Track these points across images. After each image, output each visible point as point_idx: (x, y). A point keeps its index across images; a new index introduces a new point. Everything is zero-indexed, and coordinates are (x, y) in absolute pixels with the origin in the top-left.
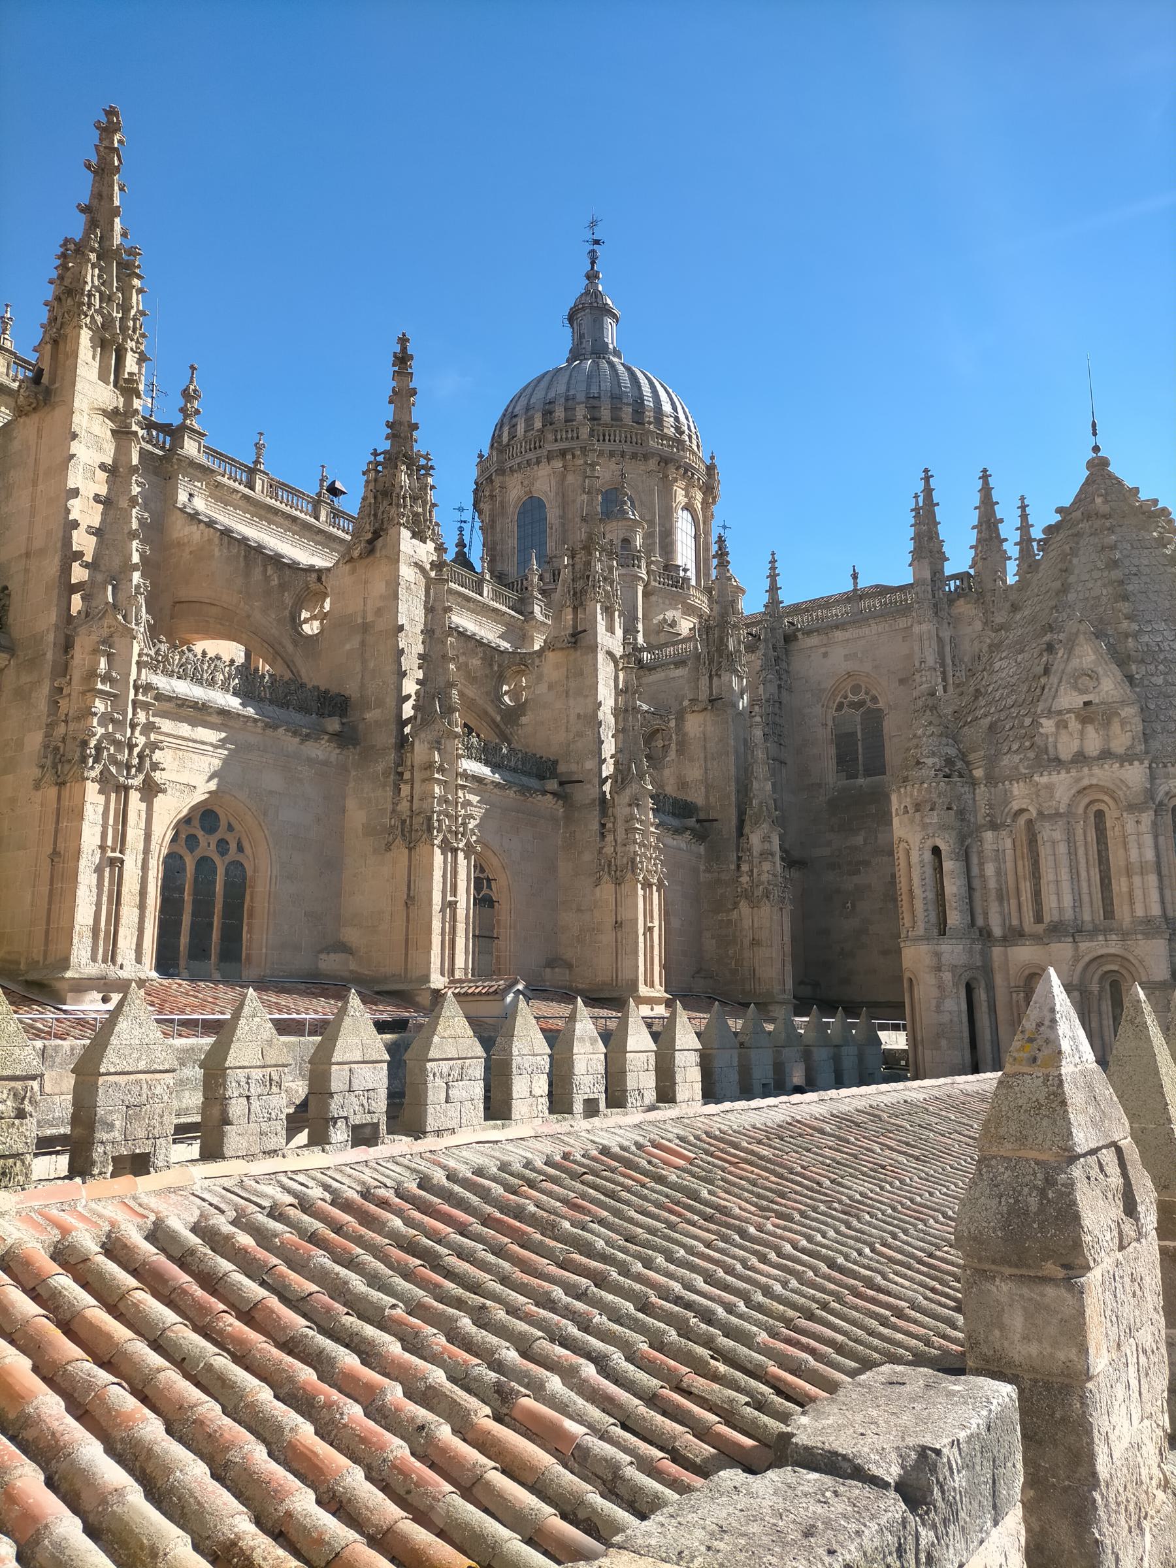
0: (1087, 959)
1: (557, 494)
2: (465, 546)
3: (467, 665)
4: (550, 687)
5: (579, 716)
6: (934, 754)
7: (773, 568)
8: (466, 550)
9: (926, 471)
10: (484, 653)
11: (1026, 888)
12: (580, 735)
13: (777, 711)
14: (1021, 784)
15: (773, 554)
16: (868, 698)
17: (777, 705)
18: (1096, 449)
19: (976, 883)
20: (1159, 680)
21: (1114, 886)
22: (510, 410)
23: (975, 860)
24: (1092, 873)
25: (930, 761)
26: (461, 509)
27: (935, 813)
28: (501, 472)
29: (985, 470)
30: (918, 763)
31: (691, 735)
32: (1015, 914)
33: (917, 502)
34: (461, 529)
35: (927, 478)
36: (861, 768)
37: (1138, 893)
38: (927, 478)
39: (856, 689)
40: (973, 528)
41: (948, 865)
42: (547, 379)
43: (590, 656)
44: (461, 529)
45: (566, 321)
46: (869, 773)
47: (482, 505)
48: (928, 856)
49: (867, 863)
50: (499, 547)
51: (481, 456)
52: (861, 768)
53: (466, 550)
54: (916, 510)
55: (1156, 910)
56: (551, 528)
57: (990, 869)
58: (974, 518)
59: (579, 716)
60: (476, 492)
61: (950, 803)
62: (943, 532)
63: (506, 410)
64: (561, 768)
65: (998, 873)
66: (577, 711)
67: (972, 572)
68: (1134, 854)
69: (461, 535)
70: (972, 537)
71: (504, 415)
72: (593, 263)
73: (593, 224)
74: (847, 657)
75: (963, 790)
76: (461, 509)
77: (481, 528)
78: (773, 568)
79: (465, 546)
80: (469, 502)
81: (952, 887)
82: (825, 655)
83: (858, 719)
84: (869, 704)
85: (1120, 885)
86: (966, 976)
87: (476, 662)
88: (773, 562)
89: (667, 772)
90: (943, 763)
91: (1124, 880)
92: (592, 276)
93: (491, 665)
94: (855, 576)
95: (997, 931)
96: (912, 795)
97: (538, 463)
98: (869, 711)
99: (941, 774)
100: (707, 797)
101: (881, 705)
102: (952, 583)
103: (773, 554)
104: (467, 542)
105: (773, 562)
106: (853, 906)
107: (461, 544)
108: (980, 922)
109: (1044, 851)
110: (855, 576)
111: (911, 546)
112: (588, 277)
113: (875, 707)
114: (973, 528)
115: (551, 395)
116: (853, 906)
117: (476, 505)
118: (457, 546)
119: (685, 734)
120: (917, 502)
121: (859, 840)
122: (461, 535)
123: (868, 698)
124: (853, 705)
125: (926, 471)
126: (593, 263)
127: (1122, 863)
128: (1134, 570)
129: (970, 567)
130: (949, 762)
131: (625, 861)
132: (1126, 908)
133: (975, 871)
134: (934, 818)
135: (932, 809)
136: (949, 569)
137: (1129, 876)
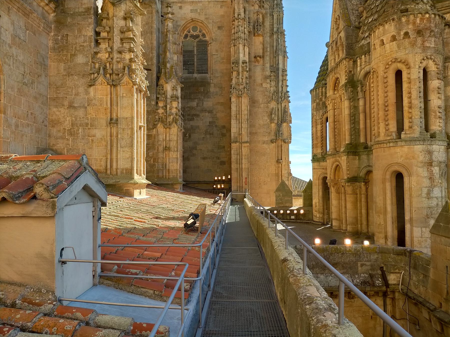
16: (200, 34)
36: (195, 69)
39: (195, 29)
46: (199, 72)
49: (198, 116)
52: (195, 69)
83: (195, 44)
84: (201, 37)
98: (200, 41)
101: (207, 38)
106: (190, 136)
113: (204, 39)
116: (190, 136)
121: (194, 104)
123: (200, 34)
124: (192, 36)
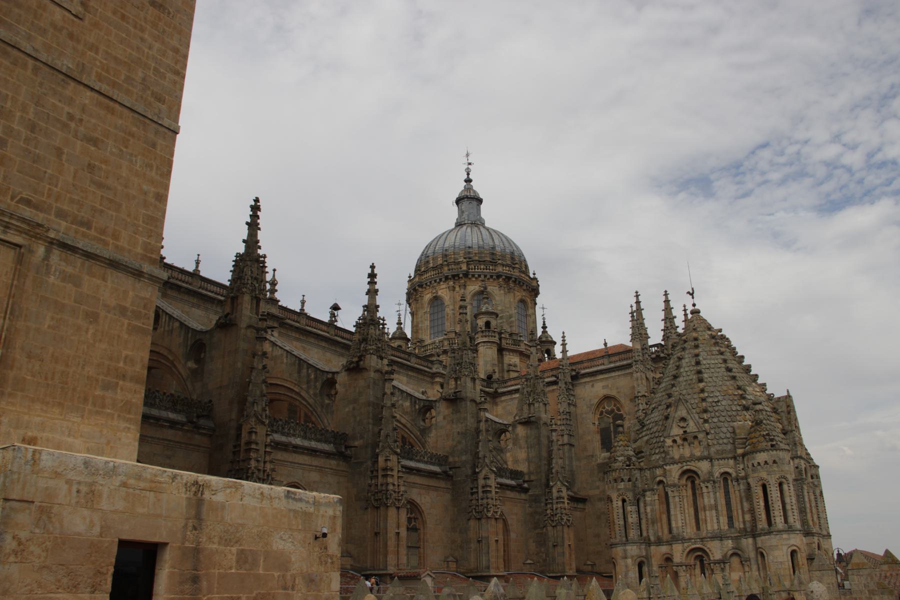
0: (688, 550)
1: (450, 298)
2: (401, 324)
3: (403, 406)
4: (444, 418)
5: (458, 433)
6: (622, 455)
7: (564, 341)
8: (402, 326)
9: (637, 292)
10: (411, 400)
11: (664, 517)
12: (459, 442)
13: (568, 417)
14: (660, 469)
15: (563, 333)
17: (568, 414)
18: (694, 305)
19: (643, 516)
20: (715, 420)
21: (700, 517)
22: (425, 253)
23: (642, 505)
24: (690, 510)
25: (620, 459)
26: (399, 304)
27: (623, 483)
28: (421, 286)
29: (666, 292)
30: (615, 460)
31: (520, 435)
32: (660, 530)
33: (632, 309)
34: (399, 315)
35: (637, 296)
37: (708, 519)
38: (637, 296)
40: (662, 320)
41: (629, 508)
42: (446, 234)
43: (463, 403)
44: (399, 315)
45: (455, 204)
47: (411, 301)
48: (620, 503)
50: (420, 325)
51: (410, 277)
53: (402, 326)
54: (632, 313)
55: (716, 527)
56: (448, 316)
57: (649, 509)
58: (662, 315)
59: (458, 433)
60: (407, 294)
61: (630, 478)
62: (647, 324)
63: (423, 253)
64: (451, 459)
65: (652, 511)
66: (458, 430)
67: (663, 343)
68: (706, 500)
69: (399, 318)
70: (662, 325)
71: (422, 255)
72: (468, 174)
73: (467, 155)
74: (604, 387)
75: (635, 472)
76: (399, 304)
77: (410, 313)
78: (564, 341)
79: (401, 324)
80: (405, 297)
81: (632, 519)
82: (593, 386)
85: (701, 515)
86: (639, 560)
87: (407, 404)
88: (563, 337)
89: (508, 454)
90: (626, 460)
91: (703, 513)
92: (468, 181)
93: (415, 406)
94: (605, 344)
95: (652, 538)
96: (612, 476)
97: (441, 280)
99: (625, 465)
100: (529, 468)
102: (653, 348)
103: (563, 333)
104: (402, 321)
105: (563, 337)
107: (399, 323)
108: (645, 534)
109: (671, 500)
110: (605, 344)
111: (630, 331)
112: (466, 181)
114: (662, 320)
115: (447, 245)
117: (408, 301)
118: (397, 324)
119: (517, 435)
120: (632, 309)
122: (399, 318)
125: (637, 292)
126: (468, 174)
127: (702, 506)
128: (708, 366)
129: (662, 340)
130: (629, 459)
131: (482, 508)
132: (704, 526)
133: (642, 510)
134: (622, 485)
135: (621, 482)
136: (651, 342)
137: (705, 511)
